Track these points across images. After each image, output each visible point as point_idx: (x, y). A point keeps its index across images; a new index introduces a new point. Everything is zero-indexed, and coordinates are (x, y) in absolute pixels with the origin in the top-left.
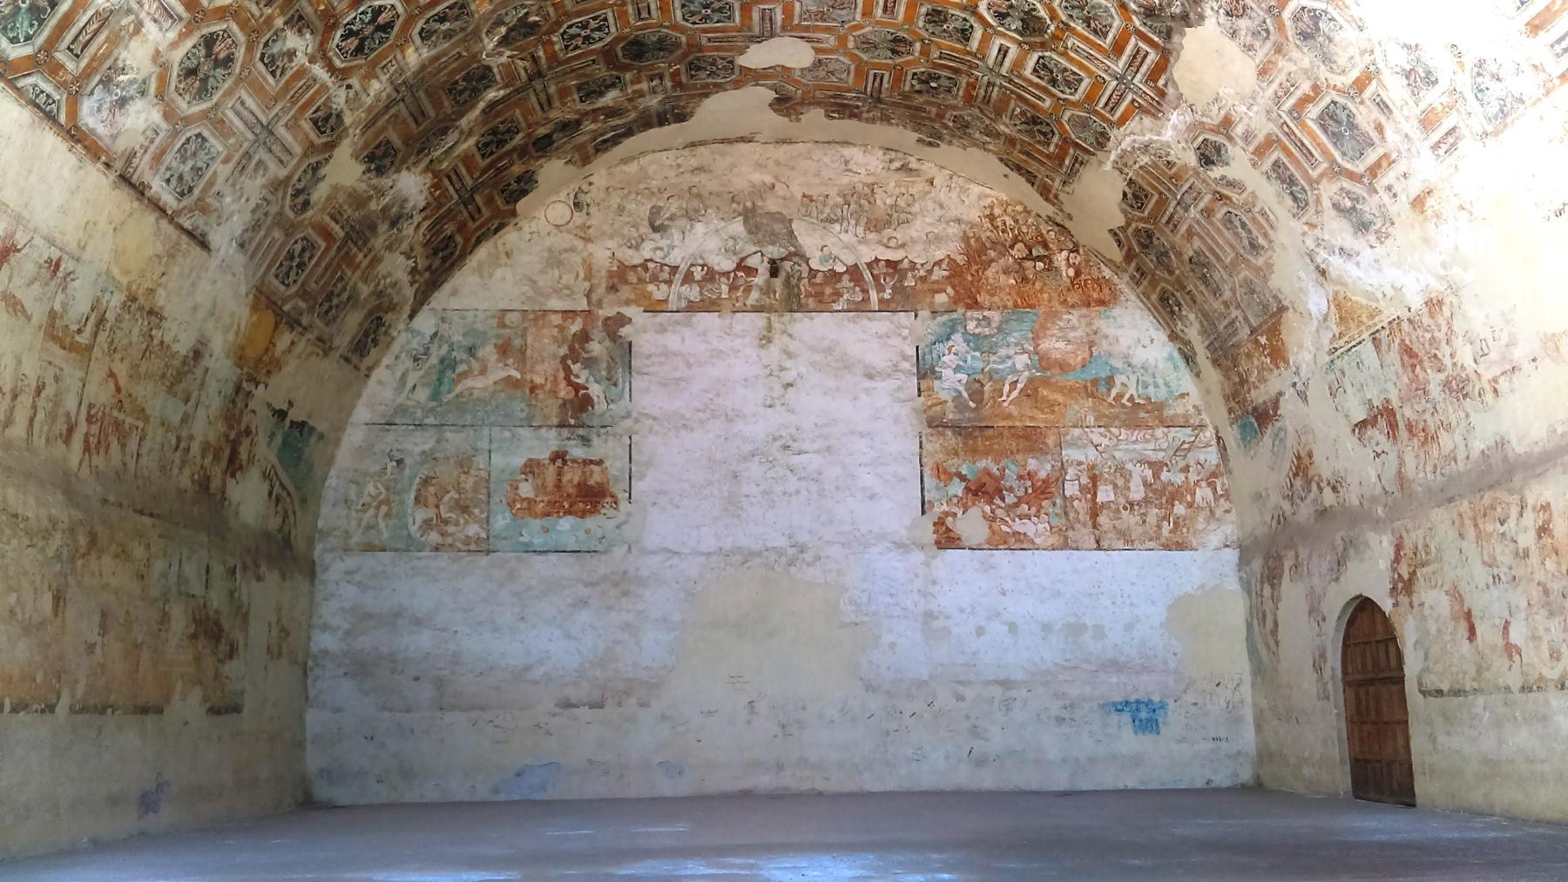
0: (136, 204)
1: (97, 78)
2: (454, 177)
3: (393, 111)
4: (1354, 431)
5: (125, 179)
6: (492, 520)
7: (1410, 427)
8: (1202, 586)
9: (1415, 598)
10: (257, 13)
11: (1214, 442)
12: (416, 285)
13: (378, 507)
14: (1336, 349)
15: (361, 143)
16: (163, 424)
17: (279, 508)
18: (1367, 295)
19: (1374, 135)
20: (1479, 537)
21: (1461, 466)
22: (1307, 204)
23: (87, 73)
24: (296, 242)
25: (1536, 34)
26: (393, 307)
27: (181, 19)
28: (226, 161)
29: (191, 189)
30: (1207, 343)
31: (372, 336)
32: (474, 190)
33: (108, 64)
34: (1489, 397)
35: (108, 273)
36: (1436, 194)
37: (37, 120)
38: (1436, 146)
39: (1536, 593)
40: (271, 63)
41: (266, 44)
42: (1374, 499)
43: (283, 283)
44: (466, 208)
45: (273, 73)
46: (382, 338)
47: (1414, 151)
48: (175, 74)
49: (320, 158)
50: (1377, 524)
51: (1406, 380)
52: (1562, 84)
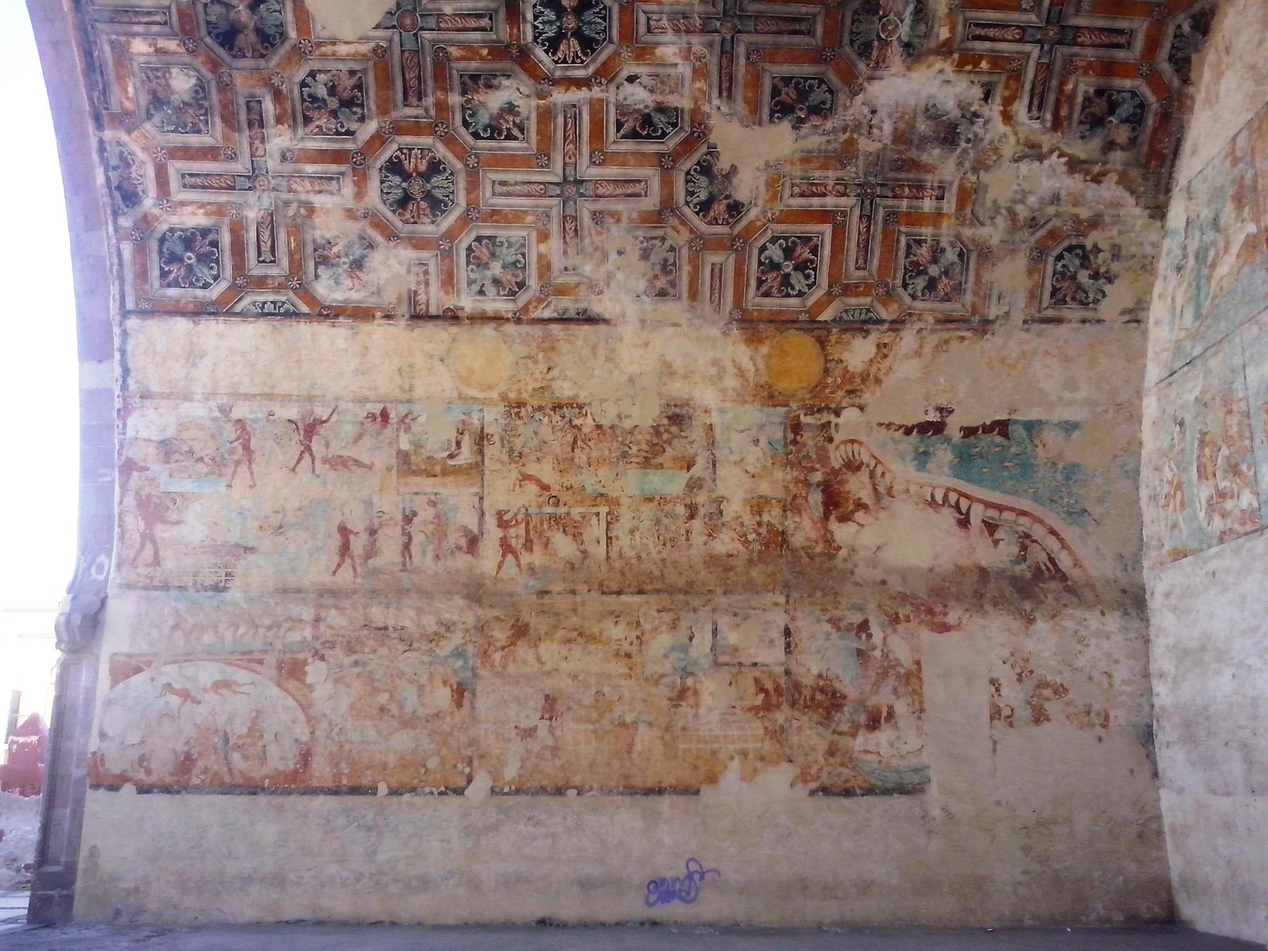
0: (454, 330)
1: (311, 265)
2: (979, 32)
3: (741, 50)
5: (419, 317)
6: (1259, 476)
10: (420, 112)
12: (1113, 177)
13: (1175, 496)
15: (740, 106)
16: (650, 500)
17: (999, 534)
23: (296, 267)
24: (763, 249)
26: (1095, 223)
27: (342, 174)
28: (544, 237)
29: (521, 285)
31: (1083, 277)
32: (1054, 18)
33: (309, 249)
35: (460, 397)
37: (277, 324)
40: (494, 131)
41: (466, 124)
43: (788, 295)
44: (1076, 44)
45: (510, 137)
46: (1115, 267)
48: (389, 214)
49: (696, 157)
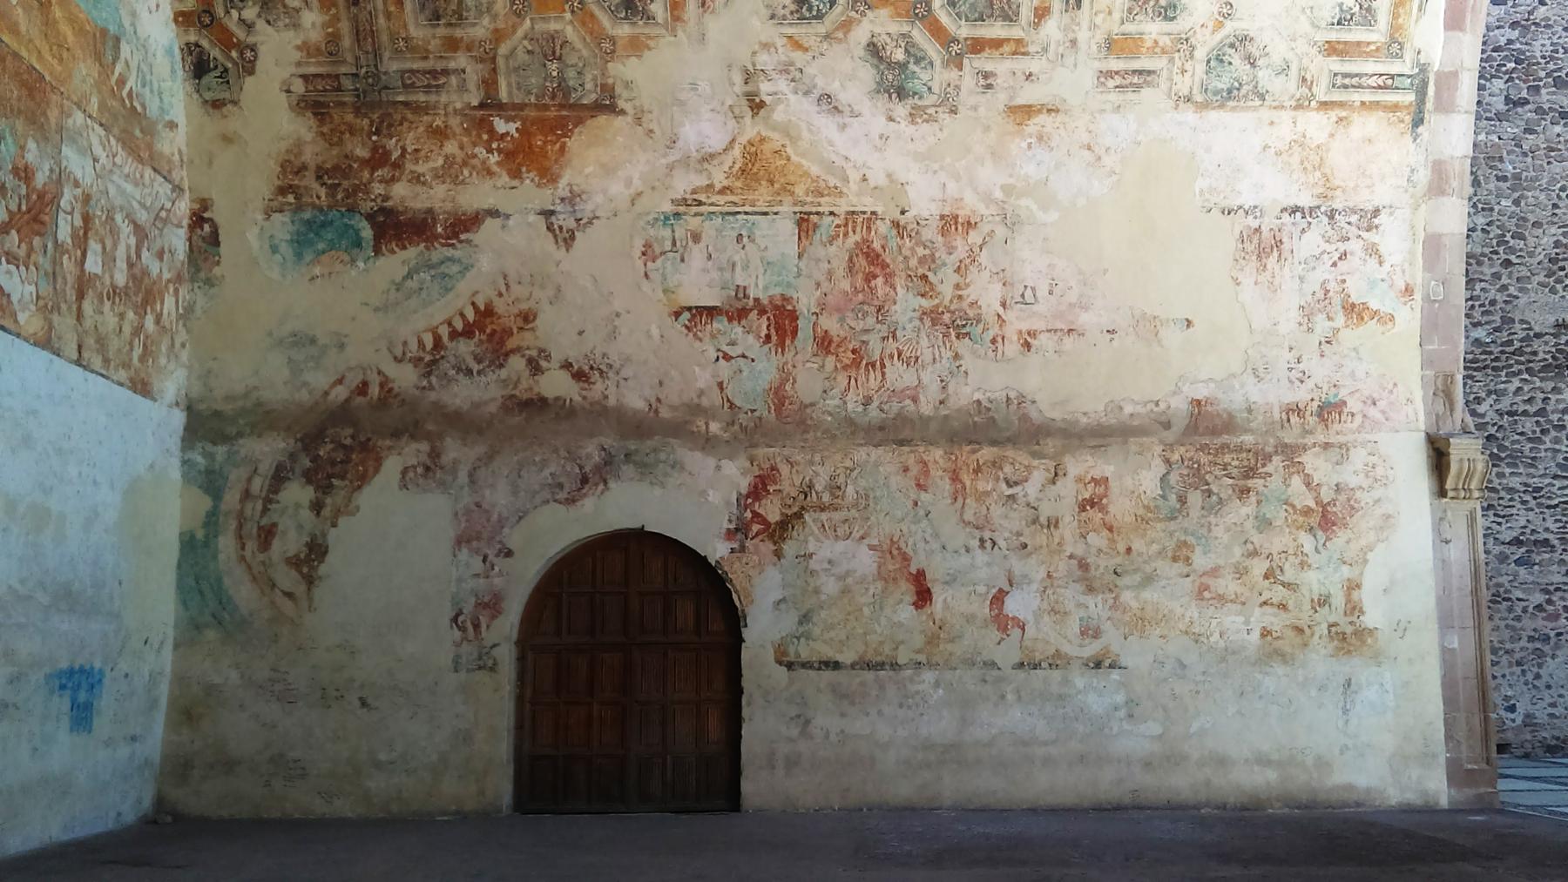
4: (677, 314)
7: (825, 343)
8: (152, 466)
9: (789, 548)
11: (185, 222)
14: (700, 203)
18: (830, 166)
19: (1026, 14)
20: (959, 494)
21: (926, 409)
22: (820, 16)
25: (1329, 55)
30: (312, 70)
34: (1012, 348)
36: (1060, 118)
38: (1110, 74)
39: (1062, 567)
42: (696, 410)
47: (1069, 60)
50: (707, 443)
51: (845, 285)
52: (1318, 109)
